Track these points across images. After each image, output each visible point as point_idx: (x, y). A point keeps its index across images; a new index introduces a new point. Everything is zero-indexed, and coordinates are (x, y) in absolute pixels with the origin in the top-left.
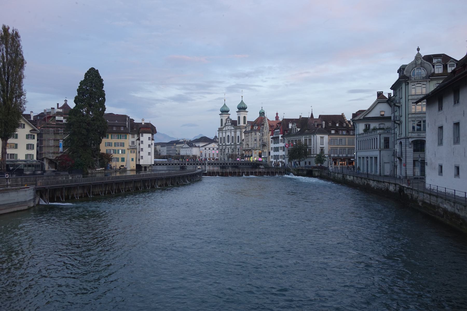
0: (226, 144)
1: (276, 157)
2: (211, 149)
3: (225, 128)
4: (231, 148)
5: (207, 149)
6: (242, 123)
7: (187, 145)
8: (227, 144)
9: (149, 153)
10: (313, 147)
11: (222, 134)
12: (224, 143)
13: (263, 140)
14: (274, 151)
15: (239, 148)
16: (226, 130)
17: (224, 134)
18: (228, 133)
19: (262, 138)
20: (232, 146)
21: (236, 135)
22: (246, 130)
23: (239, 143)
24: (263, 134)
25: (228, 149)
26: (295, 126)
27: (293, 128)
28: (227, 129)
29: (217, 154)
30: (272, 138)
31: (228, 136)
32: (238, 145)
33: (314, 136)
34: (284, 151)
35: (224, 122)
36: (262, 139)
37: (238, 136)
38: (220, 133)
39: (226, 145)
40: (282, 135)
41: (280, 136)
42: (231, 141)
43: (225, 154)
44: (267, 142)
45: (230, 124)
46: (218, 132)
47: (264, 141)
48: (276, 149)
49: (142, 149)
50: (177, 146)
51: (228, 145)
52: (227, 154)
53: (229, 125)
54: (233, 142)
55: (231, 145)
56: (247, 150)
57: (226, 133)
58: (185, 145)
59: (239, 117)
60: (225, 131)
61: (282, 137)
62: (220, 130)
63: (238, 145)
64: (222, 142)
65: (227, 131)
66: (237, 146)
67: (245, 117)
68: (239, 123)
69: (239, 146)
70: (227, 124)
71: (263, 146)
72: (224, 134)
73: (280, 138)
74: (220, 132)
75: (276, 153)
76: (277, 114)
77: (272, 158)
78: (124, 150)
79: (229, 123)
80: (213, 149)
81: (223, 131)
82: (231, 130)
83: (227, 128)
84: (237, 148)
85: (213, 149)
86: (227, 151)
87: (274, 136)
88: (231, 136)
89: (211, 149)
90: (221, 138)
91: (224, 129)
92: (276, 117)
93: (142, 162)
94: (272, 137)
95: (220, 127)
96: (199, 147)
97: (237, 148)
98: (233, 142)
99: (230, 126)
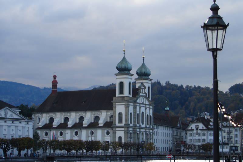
12: (138, 123)
15: (151, 134)
16: (140, 103)
25: (143, 134)
28: (141, 102)
39: (140, 128)
42: (145, 121)
51: (143, 128)
54: (148, 124)
55: (145, 128)
57: (140, 108)
76: (55, 77)
79: (142, 93)
82: (146, 104)
92: (52, 83)
99: (145, 99)
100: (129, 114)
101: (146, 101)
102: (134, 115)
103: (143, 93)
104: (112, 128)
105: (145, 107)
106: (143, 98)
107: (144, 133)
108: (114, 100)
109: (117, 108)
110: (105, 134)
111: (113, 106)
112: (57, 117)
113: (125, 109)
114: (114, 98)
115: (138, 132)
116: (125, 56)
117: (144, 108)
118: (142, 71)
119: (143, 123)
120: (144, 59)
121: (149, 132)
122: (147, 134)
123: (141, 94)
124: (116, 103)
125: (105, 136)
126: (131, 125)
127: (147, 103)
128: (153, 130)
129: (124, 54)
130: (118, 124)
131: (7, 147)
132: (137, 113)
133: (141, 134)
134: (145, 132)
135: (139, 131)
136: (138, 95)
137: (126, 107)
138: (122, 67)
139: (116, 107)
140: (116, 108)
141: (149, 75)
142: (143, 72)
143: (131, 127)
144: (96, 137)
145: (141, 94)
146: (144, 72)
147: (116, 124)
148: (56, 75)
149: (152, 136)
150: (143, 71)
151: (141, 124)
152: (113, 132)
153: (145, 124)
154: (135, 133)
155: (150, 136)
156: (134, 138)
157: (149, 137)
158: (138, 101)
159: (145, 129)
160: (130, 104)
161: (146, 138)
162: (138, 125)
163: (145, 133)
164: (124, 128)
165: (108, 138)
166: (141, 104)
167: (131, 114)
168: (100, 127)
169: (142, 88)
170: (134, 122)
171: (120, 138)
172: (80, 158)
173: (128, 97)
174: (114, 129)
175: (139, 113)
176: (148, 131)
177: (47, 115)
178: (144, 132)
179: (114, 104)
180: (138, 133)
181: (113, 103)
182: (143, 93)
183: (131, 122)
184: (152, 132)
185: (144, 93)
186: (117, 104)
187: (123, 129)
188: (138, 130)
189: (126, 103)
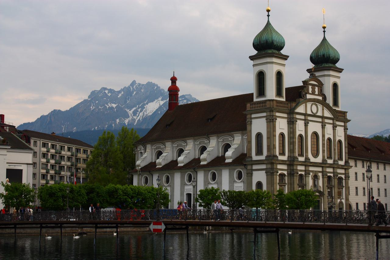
0: (307, 159)
8: (313, 160)
12: (301, 155)
15: (343, 176)
16: (305, 115)
18: (314, 127)
25: (316, 177)
28: (309, 112)
39: (307, 163)
51: (315, 165)
54: (330, 157)
55: (323, 164)
57: (306, 125)
79: (313, 93)
81: (298, 116)
82: (323, 117)
88: (323, 136)
92: (170, 89)
99: (320, 107)
100: (275, 136)
101: (323, 109)
102: (290, 138)
103: (317, 93)
104: (245, 165)
105: (322, 122)
106: (317, 105)
107: (320, 175)
108: (247, 110)
109: (253, 126)
110: (235, 179)
111: (247, 121)
112: (166, 149)
113: (267, 125)
114: (248, 105)
115: (303, 173)
116: (271, 22)
117: (320, 124)
118: (319, 54)
120: (324, 32)
121: (333, 173)
122: (329, 177)
123: (309, 96)
124: (251, 114)
125: (235, 182)
126: (285, 158)
127: (327, 114)
128: (345, 169)
129: (268, 16)
130: (255, 158)
131: (14, 204)
132: (298, 133)
133: (310, 178)
134: (322, 172)
135: (305, 171)
136: (301, 98)
137: (268, 120)
138: (262, 42)
139: (251, 122)
140: (251, 124)
141: (336, 60)
142: (322, 53)
143: (283, 162)
144: (220, 183)
145: (309, 96)
146: (324, 55)
147: (251, 157)
149: (344, 180)
150: (321, 52)
151: (310, 156)
152: (247, 174)
153: (323, 157)
154: (293, 174)
155: (336, 181)
156: (291, 184)
157: (335, 182)
158: (301, 109)
159: (323, 167)
160: (278, 114)
161: (326, 184)
162: (302, 159)
163: (323, 176)
164: (266, 164)
165: (239, 187)
166: (310, 115)
167: (282, 135)
168: (229, 164)
169: (313, 86)
170: (292, 151)
171: (259, 184)
172: (15, 228)
173: (276, 100)
174: (249, 167)
175: (303, 134)
176: (331, 170)
177: (153, 148)
178: (320, 172)
179: (248, 116)
180: (301, 175)
181: (246, 115)
182: (317, 93)
183: (283, 153)
184: (345, 174)
185: (318, 95)
186: (253, 116)
187: (264, 167)
188: (300, 168)
189: (269, 114)
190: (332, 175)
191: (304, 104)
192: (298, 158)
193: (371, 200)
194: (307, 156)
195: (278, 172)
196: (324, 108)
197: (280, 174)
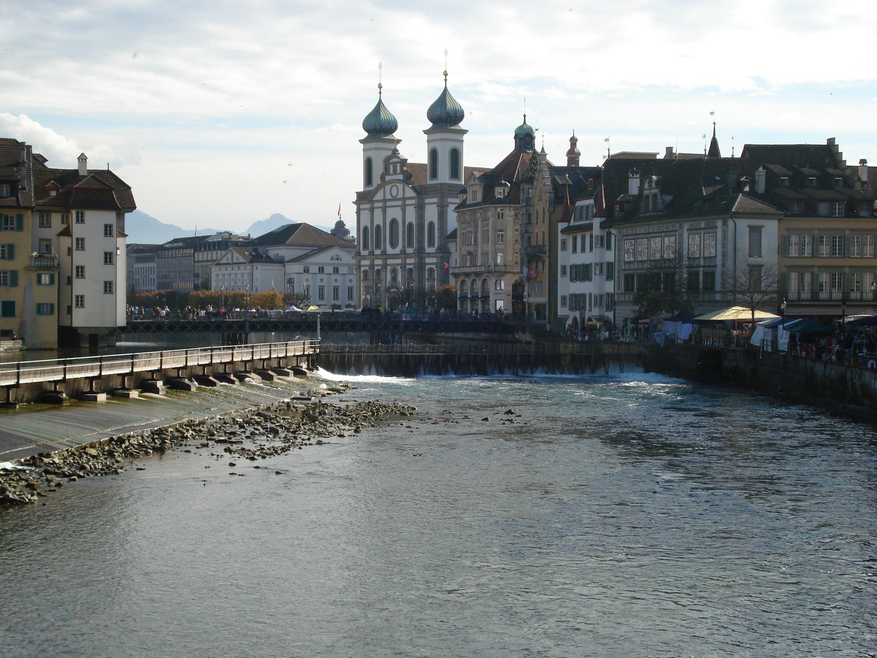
1: (578, 301)
2: (329, 270)
3: (381, 192)
4: (403, 266)
5: (314, 269)
6: (444, 176)
7: (236, 255)
8: (390, 250)
9: (106, 283)
10: (723, 265)
11: (372, 210)
13: (529, 238)
14: (571, 280)
15: (434, 267)
16: (385, 201)
17: (378, 214)
18: (394, 213)
19: (527, 232)
20: (409, 261)
21: (421, 216)
22: (465, 201)
23: (432, 250)
24: (529, 215)
25: (394, 271)
26: (654, 185)
27: (646, 192)
28: (388, 197)
29: (350, 289)
30: (563, 231)
31: (394, 222)
32: (429, 255)
33: (725, 223)
34: (609, 277)
35: (378, 169)
36: (526, 236)
37: (431, 224)
38: (361, 212)
40: (604, 219)
41: (596, 222)
42: (404, 239)
43: (383, 289)
44: (547, 243)
45: (401, 177)
46: (355, 207)
47: (534, 243)
48: (582, 273)
49: (81, 271)
50: (201, 256)
51: (394, 256)
52: (390, 288)
53: (399, 181)
54: (410, 244)
55: (404, 254)
56: (467, 275)
58: (229, 255)
59: (433, 155)
60: (381, 204)
61: (602, 226)
62: (361, 198)
63: (429, 255)
64: (371, 242)
65: (388, 204)
66: (428, 260)
67: (456, 156)
68: (434, 175)
69: (434, 260)
70: (388, 178)
71: (529, 262)
72: (378, 214)
73: (596, 231)
74: (362, 207)
75: (579, 288)
76: (573, 141)
77: (564, 304)
78: (14, 274)
79: (395, 172)
80: (336, 271)
81: (376, 205)
82: (404, 199)
83: (388, 192)
84: (427, 267)
85: (336, 271)
86: (389, 278)
87: (572, 223)
89: (329, 270)
90: (366, 229)
91: (379, 196)
93: (80, 319)
94: (565, 225)
95: (361, 189)
96: (281, 261)
97: (427, 267)
98: (410, 244)
99: (400, 186)
101: (404, 190)
103: (399, 171)
107: (399, 267)
119: (393, 245)
120: (446, 80)
148: (575, 136)
149: (436, 272)
153: (404, 246)
178: (398, 265)
182: (399, 171)
190: (412, 267)
191: (382, 189)
192: (373, 252)
193: (363, 297)
194: (385, 248)
195: (360, 269)
196: (406, 187)
197: (363, 271)
